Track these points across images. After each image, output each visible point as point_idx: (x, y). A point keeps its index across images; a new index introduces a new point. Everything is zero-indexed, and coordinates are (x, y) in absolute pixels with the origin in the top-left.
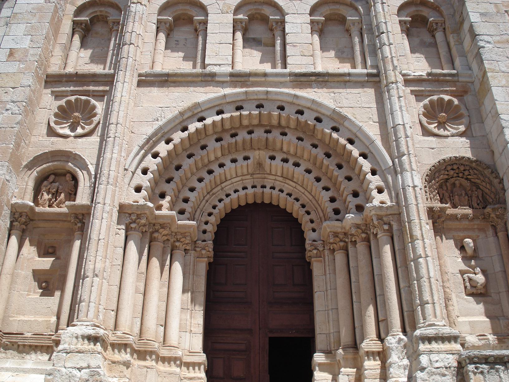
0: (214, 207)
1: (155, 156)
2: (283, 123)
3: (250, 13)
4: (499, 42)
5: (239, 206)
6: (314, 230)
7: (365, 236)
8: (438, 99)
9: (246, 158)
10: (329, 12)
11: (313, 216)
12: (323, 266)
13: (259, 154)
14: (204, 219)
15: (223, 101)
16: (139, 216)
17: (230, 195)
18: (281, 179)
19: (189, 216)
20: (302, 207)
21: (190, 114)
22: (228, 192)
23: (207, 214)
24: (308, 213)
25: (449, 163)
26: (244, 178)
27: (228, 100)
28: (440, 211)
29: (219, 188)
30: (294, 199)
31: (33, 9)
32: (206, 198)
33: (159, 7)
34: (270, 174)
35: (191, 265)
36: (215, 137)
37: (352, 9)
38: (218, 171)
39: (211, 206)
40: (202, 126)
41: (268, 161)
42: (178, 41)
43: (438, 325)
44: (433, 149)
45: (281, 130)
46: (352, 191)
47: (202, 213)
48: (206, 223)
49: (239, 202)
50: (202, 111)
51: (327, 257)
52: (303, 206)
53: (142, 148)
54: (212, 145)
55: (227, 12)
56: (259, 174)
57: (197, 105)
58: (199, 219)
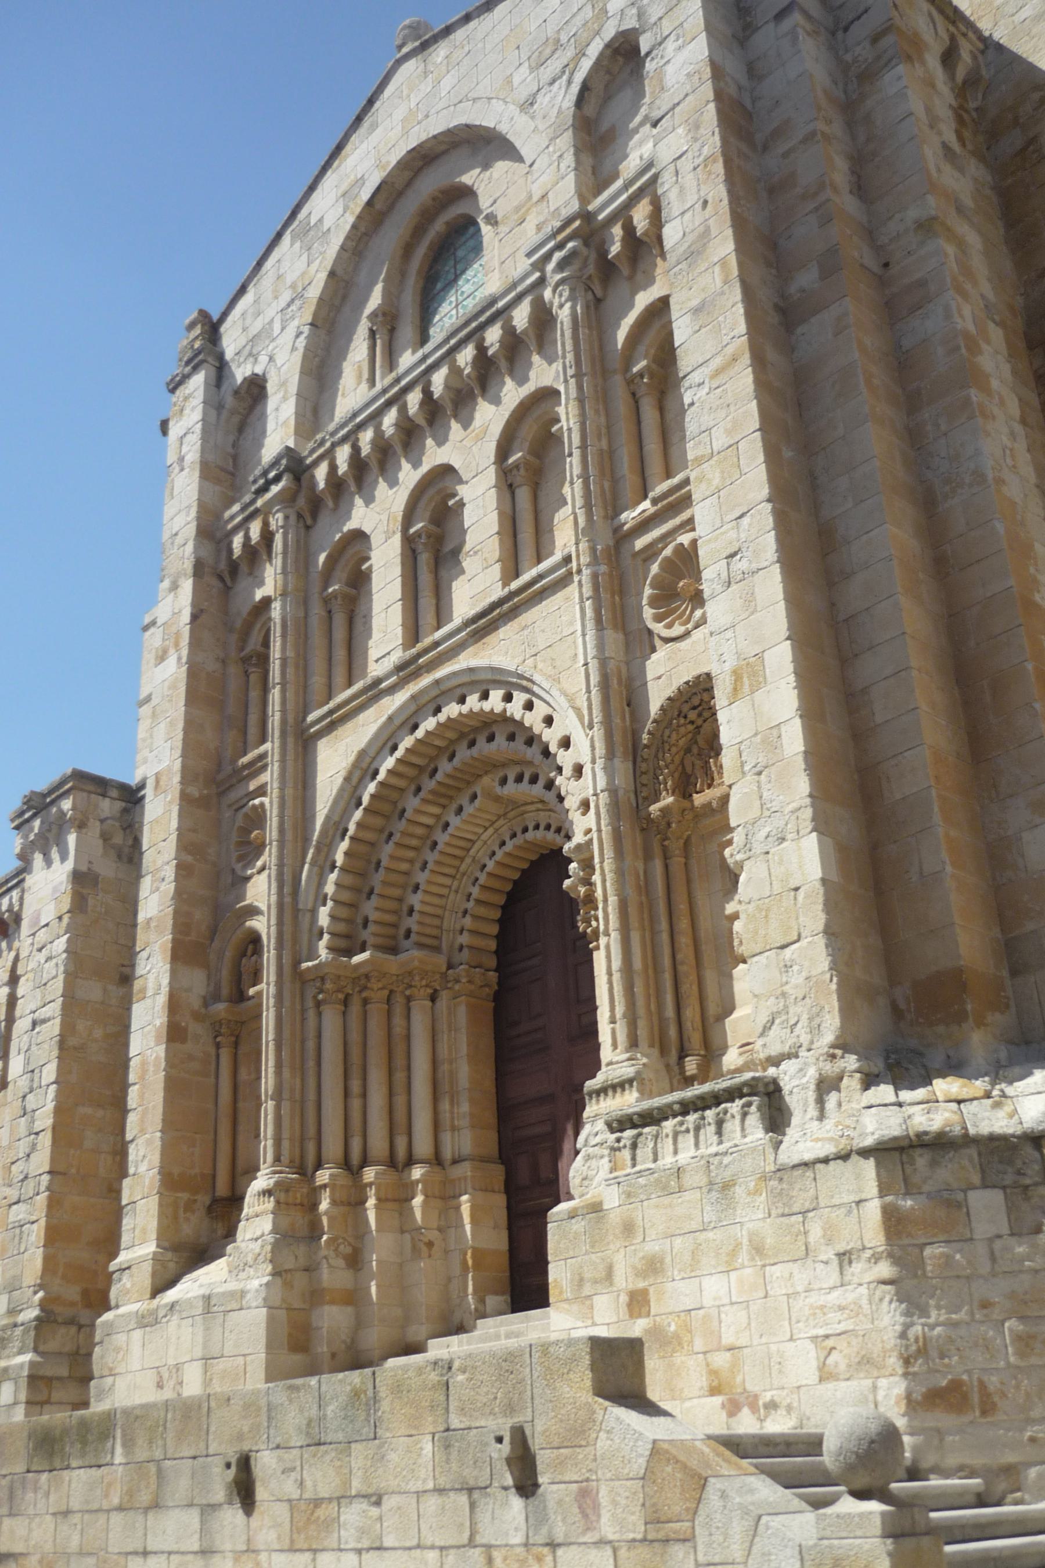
3: (433, 504)
4: (717, 373)
9: (474, 797)
14: (458, 927)
15: (393, 727)
16: (323, 979)
21: (357, 774)
22: (483, 862)
25: (683, 699)
27: (397, 722)
28: (664, 817)
29: (468, 860)
31: (169, 688)
32: (454, 888)
38: (442, 838)
40: (376, 787)
43: (617, 1063)
44: (659, 678)
45: (486, 734)
50: (374, 758)
54: (412, 803)
57: (362, 753)
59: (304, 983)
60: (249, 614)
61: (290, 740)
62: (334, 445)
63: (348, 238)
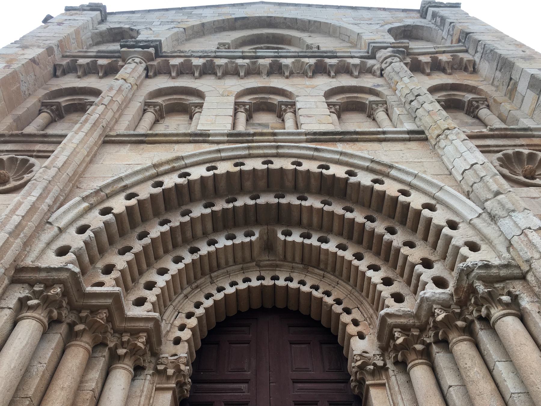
0: (198, 305)
1: (105, 212)
2: (301, 183)
5: (239, 312)
6: (361, 336)
7: (464, 326)
8: (514, 153)
10: (345, 100)
11: (356, 314)
12: (390, 396)
13: (267, 233)
14: (178, 323)
17: (224, 289)
18: (301, 266)
19: (150, 307)
20: (336, 303)
22: (220, 285)
23: (184, 315)
24: (348, 311)
26: (245, 265)
30: (323, 293)
32: (185, 292)
33: (148, 92)
34: (285, 259)
35: (143, 398)
36: (204, 202)
37: (372, 96)
39: (192, 305)
41: (282, 237)
42: (168, 126)
44: (534, 198)
46: (421, 260)
47: (177, 313)
48: (182, 328)
49: (238, 305)
50: (186, 166)
51: (393, 378)
52: (339, 302)
53: (84, 199)
55: (228, 96)
56: (269, 260)
58: (171, 322)
59: (14, 281)
60: (66, 89)
61: (96, 134)
62: (191, 56)
63: (218, 21)
